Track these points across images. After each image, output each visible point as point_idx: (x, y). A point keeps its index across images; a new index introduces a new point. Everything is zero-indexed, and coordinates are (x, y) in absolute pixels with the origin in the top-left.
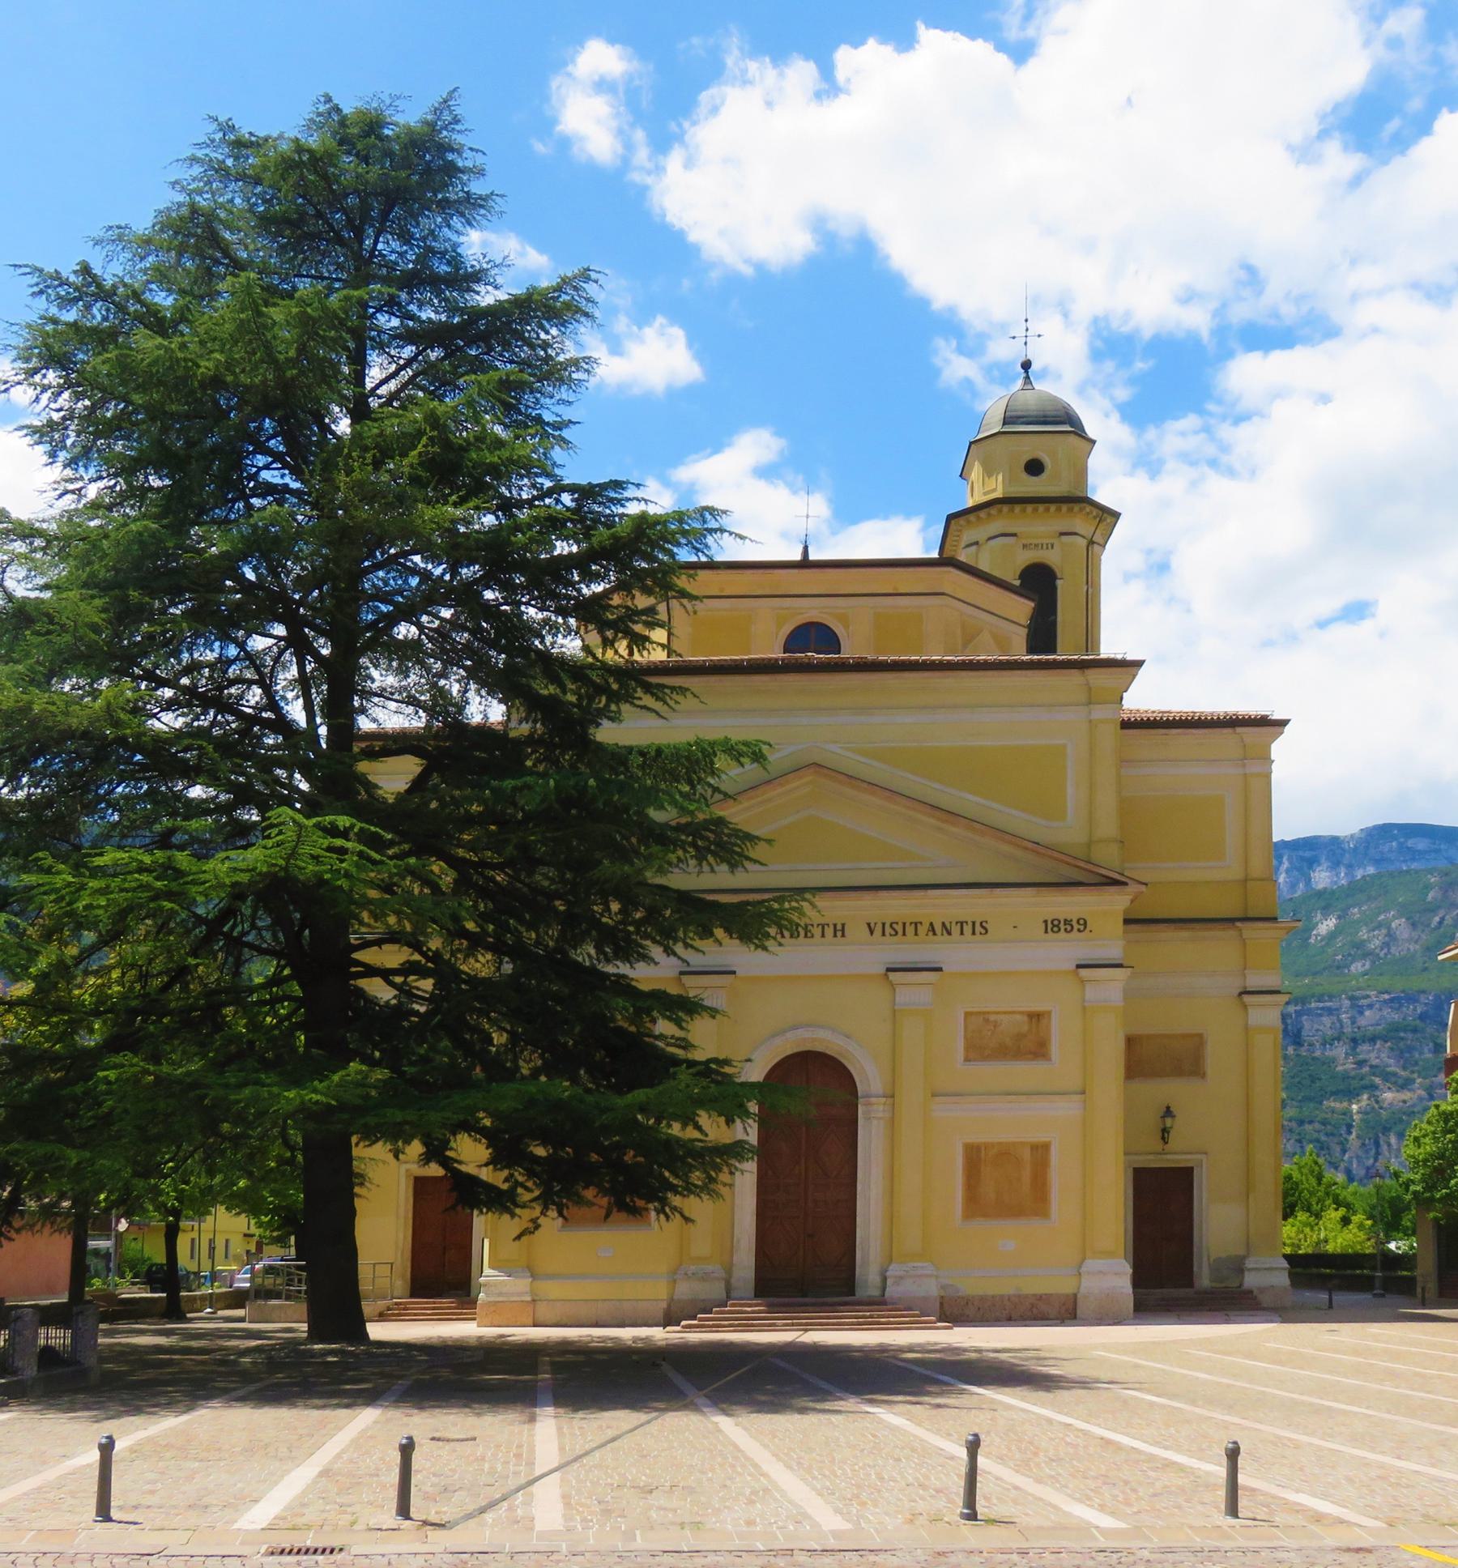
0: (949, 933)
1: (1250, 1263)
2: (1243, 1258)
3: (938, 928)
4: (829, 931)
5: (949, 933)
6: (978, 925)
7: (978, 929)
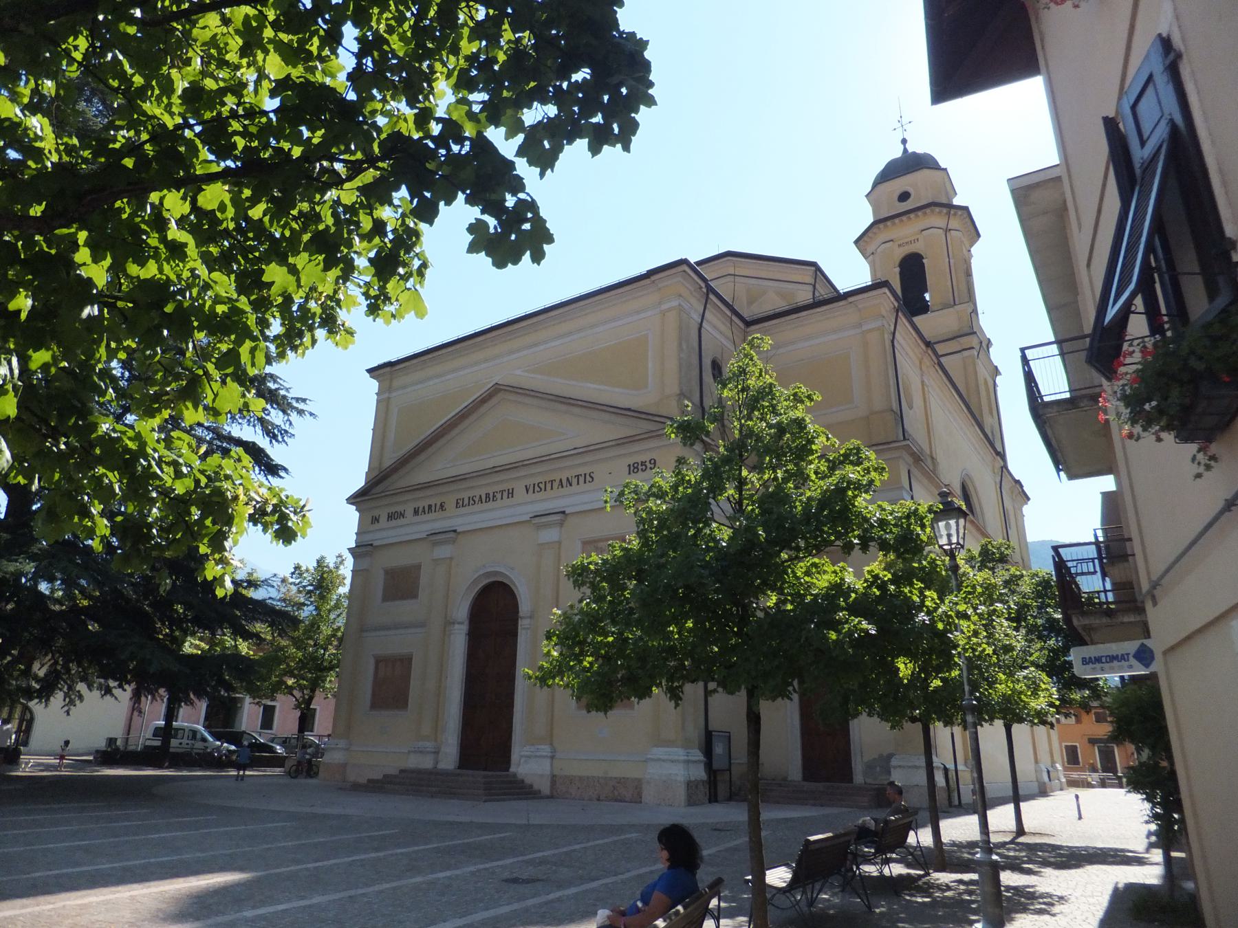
0: (571, 485)
1: (894, 762)
2: (890, 756)
3: (564, 482)
4: (505, 494)
5: (571, 485)
6: (588, 476)
7: (588, 478)
